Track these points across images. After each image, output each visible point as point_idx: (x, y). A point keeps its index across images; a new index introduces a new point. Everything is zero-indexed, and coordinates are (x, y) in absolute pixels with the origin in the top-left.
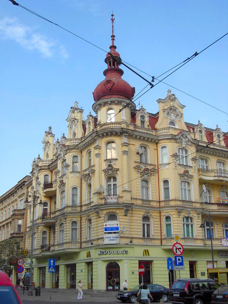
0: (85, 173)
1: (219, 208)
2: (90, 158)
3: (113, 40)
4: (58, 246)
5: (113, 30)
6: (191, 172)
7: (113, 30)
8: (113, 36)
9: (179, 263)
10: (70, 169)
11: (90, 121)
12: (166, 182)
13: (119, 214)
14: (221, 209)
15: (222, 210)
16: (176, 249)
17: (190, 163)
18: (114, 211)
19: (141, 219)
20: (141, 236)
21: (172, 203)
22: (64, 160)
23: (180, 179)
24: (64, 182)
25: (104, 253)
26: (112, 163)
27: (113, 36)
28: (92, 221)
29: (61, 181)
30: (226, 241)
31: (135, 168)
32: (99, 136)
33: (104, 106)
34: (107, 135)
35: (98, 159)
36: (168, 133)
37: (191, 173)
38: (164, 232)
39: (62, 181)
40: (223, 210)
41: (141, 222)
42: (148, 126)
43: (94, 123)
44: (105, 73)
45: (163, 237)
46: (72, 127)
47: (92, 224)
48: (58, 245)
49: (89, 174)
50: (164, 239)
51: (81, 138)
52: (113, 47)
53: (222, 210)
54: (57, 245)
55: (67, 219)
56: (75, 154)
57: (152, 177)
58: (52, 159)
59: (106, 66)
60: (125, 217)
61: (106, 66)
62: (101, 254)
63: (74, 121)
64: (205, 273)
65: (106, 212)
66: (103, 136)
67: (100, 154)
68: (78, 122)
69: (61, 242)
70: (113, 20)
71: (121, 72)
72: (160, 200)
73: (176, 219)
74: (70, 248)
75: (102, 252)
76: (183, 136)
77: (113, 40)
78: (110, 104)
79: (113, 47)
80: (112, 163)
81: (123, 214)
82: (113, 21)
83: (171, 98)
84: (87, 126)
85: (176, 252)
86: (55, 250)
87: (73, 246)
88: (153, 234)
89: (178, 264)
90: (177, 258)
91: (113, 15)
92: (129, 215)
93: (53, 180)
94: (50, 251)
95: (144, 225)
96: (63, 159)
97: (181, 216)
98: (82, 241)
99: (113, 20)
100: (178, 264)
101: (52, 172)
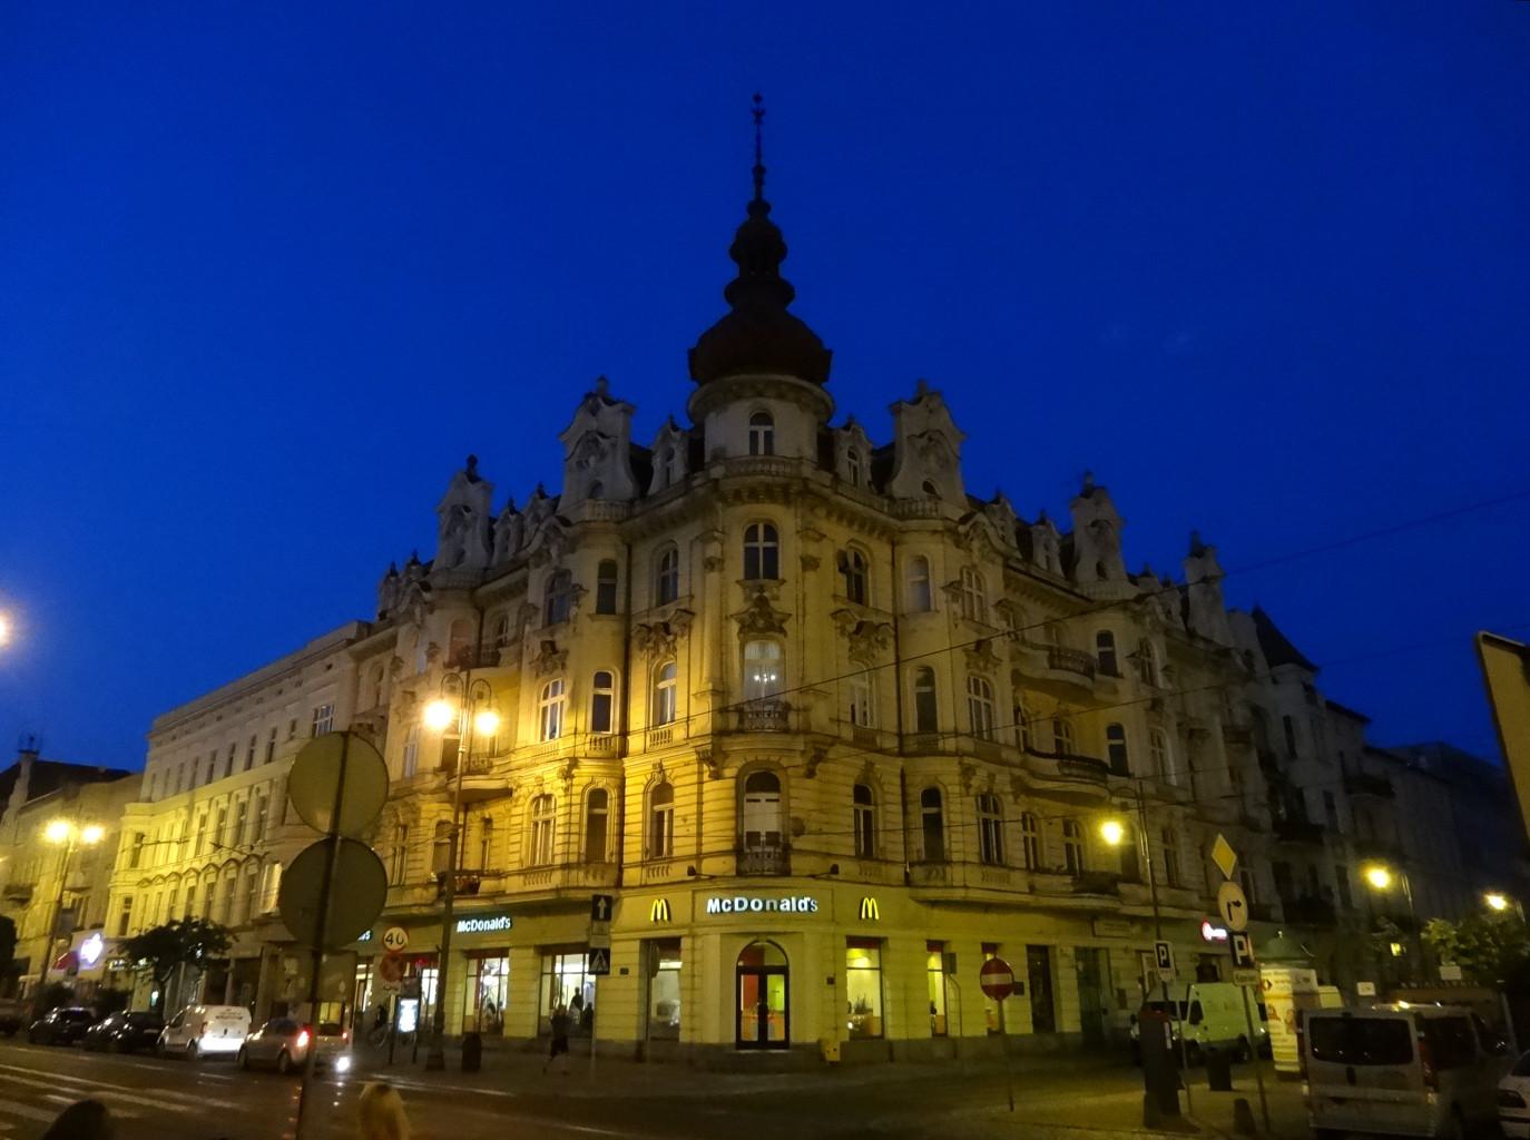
0: (644, 621)
1: (1066, 771)
2: (663, 574)
3: (759, 182)
4: (522, 878)
9: (1242, 958)
10: (590, 601)
11: (674, 446)
12: (928, 676)
14: (1070, 775)
16: (1229, 906)
18: (772, 758)
19: (850, 791)
20: (853, 853)
22: (562, 575)
23: (968, 664)
24: (560, 646)
25: (737, 908)
26: (766, 594)
28: (677, 792)
29: (548, 646)
31: (834, 615)
32: (723, 499)
33: (739, 397)
34: (754, 495)
35: (713, 577)
36: (934, 514)
37: (995, 651)
38: (919, 840)
39: (552, 644)
40: (1079, 779)
41: (851, 801)
42: (869, 483)
43: (686, 456)
44: (731, 293)
45: (915, 857)
46: (587, 462)
47: (677, 801)
48: (520, 873)
49: (666, 627)
50: (921, 863)
51: (631, 502)
52: (759, 207)
54: (519, 874)
55: (575, 781)
56: (609, 554)
58: (486, 569)
59: (732, 271)
61: (732, 271)
62: (722, 911)
63: (596, 441)
65: (744, 762)
66: (737, 495)
67: (721, 561)
68: (614, 446)
69: (537, 864)
70: (759, 114)
71: (787, 292)
72: (904, 732)
74: (581, 884)
75: (727, 905)
76: (975, 531)
77: (759, 182)
78: (760, 395)
79: (759, 207)
81: (802, 771)
84: (657, 462)
85: (1231, 919)
86: (507, 892)
87: (591, 878)
88: (881, 844)
89: (1239, 962)
90: (1237, 939)
93: (484, 642)
94: (479, 895)
95: (857, 811)
96: (556, 568)
98: (625, 862)
99: (759, 114)
100: (1239, 962)
101: (482, 612)
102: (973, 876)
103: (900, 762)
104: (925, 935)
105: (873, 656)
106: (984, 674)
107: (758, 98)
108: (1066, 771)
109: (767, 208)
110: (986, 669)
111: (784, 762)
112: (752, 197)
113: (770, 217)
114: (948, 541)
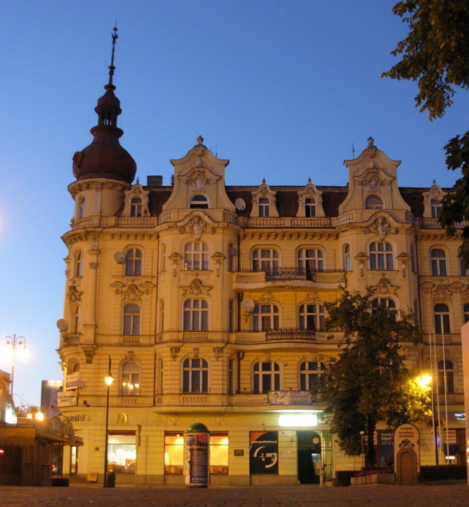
3: (111, 73)
5: (113, 56)
6: (209, 279)
7: (113, 56)
8: (112, 68)
13: (81, 362)
15: (274, 341)
17: (212, 264)
21: (166, 337)
27: (112, 68)
30: (276, 395)
42: (146, 212)
52: (110, 88)
53: (274, 341)
57: (144, 297)
60: (89, 366)
64: (243, 451)
70: (115, 37)
73: (168, 363)
77: (111, 73)
79: (110, 88)
80: (76, 285)
81: (85, 361)
82: (114, 42)
83: (197, 153)
91: (116, 29)
92: (94, 361)
97: (179, 359)
99: (115, 37)
102: (177, 400)
103: (151, 349)
104: (163, 428)
105: (140, 299)
106: (199, 296)
107: (116, 29)
108: (269, 337)
109: (114, 88)
110: (201, 293)
111: (78, 358)
112: (107, 83)
113: (114, 91)
114: (176, 231)
